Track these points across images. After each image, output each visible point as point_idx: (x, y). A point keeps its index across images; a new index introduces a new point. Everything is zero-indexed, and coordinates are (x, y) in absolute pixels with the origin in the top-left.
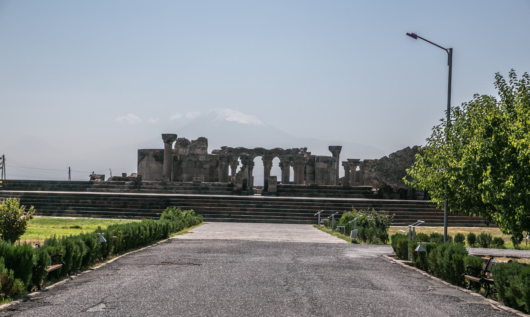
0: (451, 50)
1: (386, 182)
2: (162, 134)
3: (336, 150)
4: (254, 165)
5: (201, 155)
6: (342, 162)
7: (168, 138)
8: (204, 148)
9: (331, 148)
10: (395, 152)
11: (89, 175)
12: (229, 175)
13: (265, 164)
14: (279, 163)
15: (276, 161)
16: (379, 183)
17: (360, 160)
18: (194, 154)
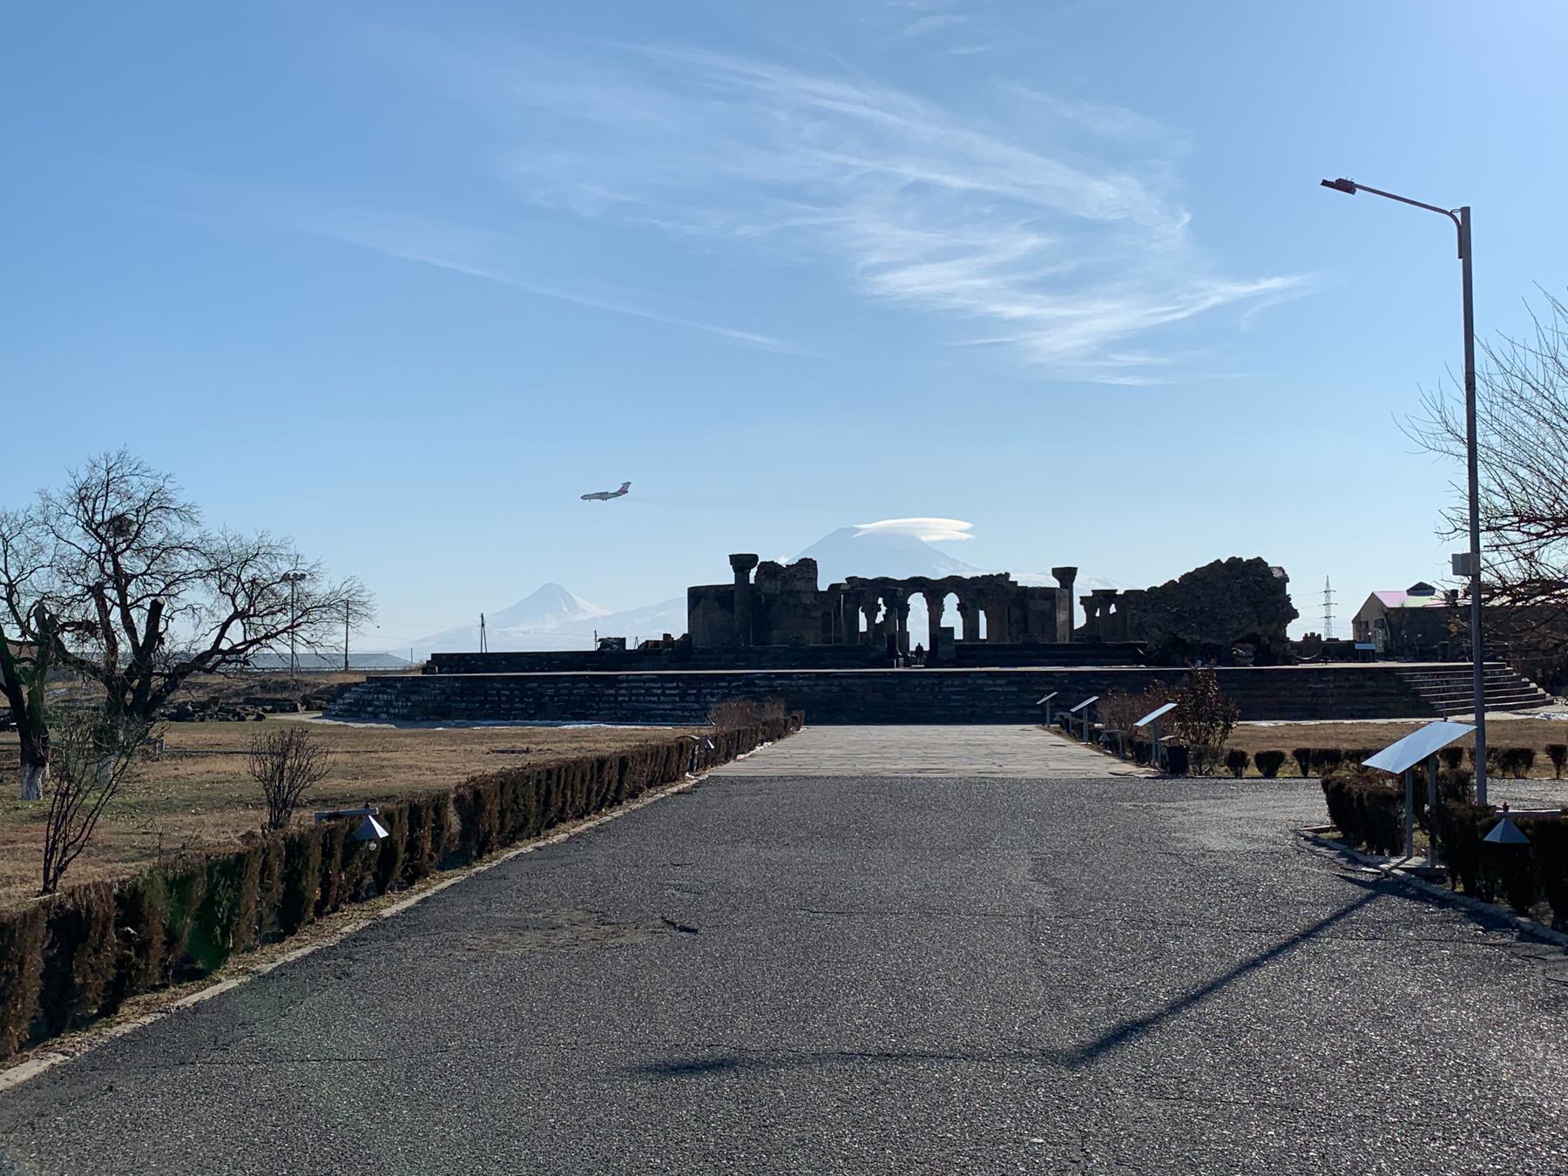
0: (1466, 211)
1: (1175, 632)
2: (730, 556)
3: (1066, 575)
4: (909, 610)
5: (806, 592)
6: (1081, 597)
7: (741, 563)
8: (810, 578)
9: (1057, 573)
10: (1191, 571)
12: (861, 630)
15: (951, 601)
16: (1161, 634)
17: (1116, 591)
18: (792, 592)
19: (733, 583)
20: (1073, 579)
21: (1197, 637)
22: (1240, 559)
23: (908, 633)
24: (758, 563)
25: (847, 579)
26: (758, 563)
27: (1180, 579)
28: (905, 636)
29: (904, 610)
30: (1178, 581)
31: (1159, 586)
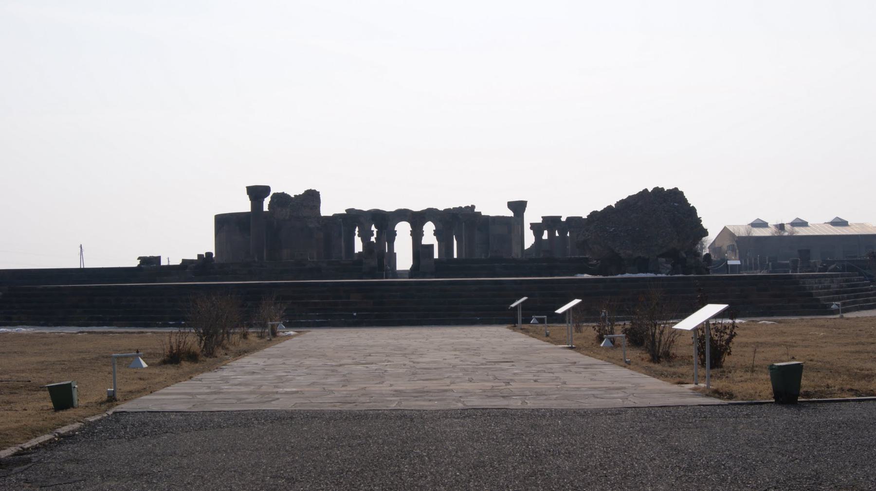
3: (518, 207)
4: (396, 235)
6: (531, 224)
7: (257, 193)
8: (314, 206)
9: (512, 205)
11: (137, 258)
13: (413, 234)
14: (434, 230)
15: (429, 228)
17: (561, 217)
19: (250, 211)
20: (524, 210)
21: (630, 252)
22: (662, 189)
23: (395, 253)
24: (271, 194)
25: (346, 211)
26: (271, 194)
27: (615, 205)
28: (392, 256)
29: (391, 236)
30: (614, 206)
31: (599, 210)
